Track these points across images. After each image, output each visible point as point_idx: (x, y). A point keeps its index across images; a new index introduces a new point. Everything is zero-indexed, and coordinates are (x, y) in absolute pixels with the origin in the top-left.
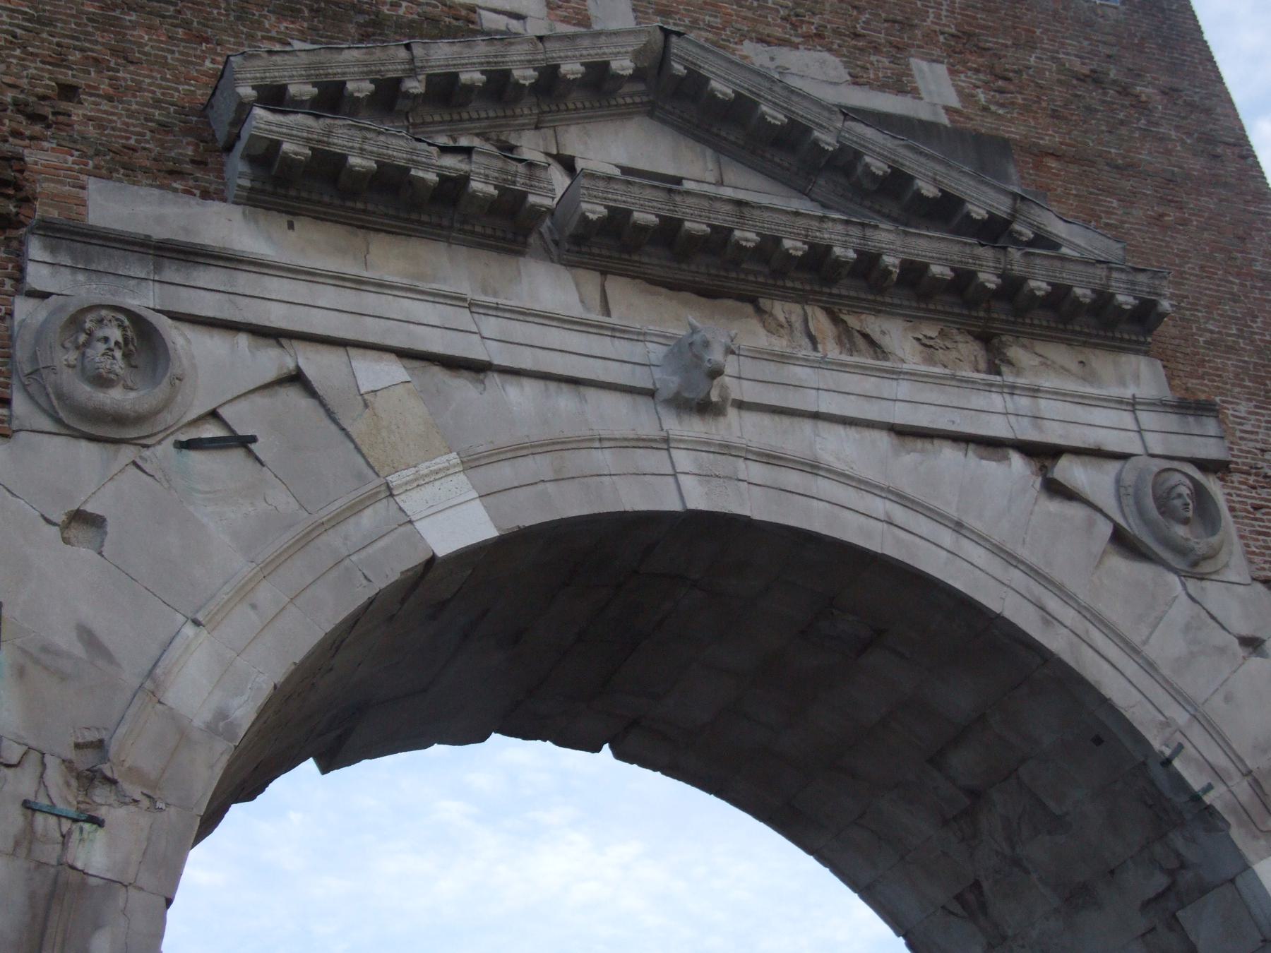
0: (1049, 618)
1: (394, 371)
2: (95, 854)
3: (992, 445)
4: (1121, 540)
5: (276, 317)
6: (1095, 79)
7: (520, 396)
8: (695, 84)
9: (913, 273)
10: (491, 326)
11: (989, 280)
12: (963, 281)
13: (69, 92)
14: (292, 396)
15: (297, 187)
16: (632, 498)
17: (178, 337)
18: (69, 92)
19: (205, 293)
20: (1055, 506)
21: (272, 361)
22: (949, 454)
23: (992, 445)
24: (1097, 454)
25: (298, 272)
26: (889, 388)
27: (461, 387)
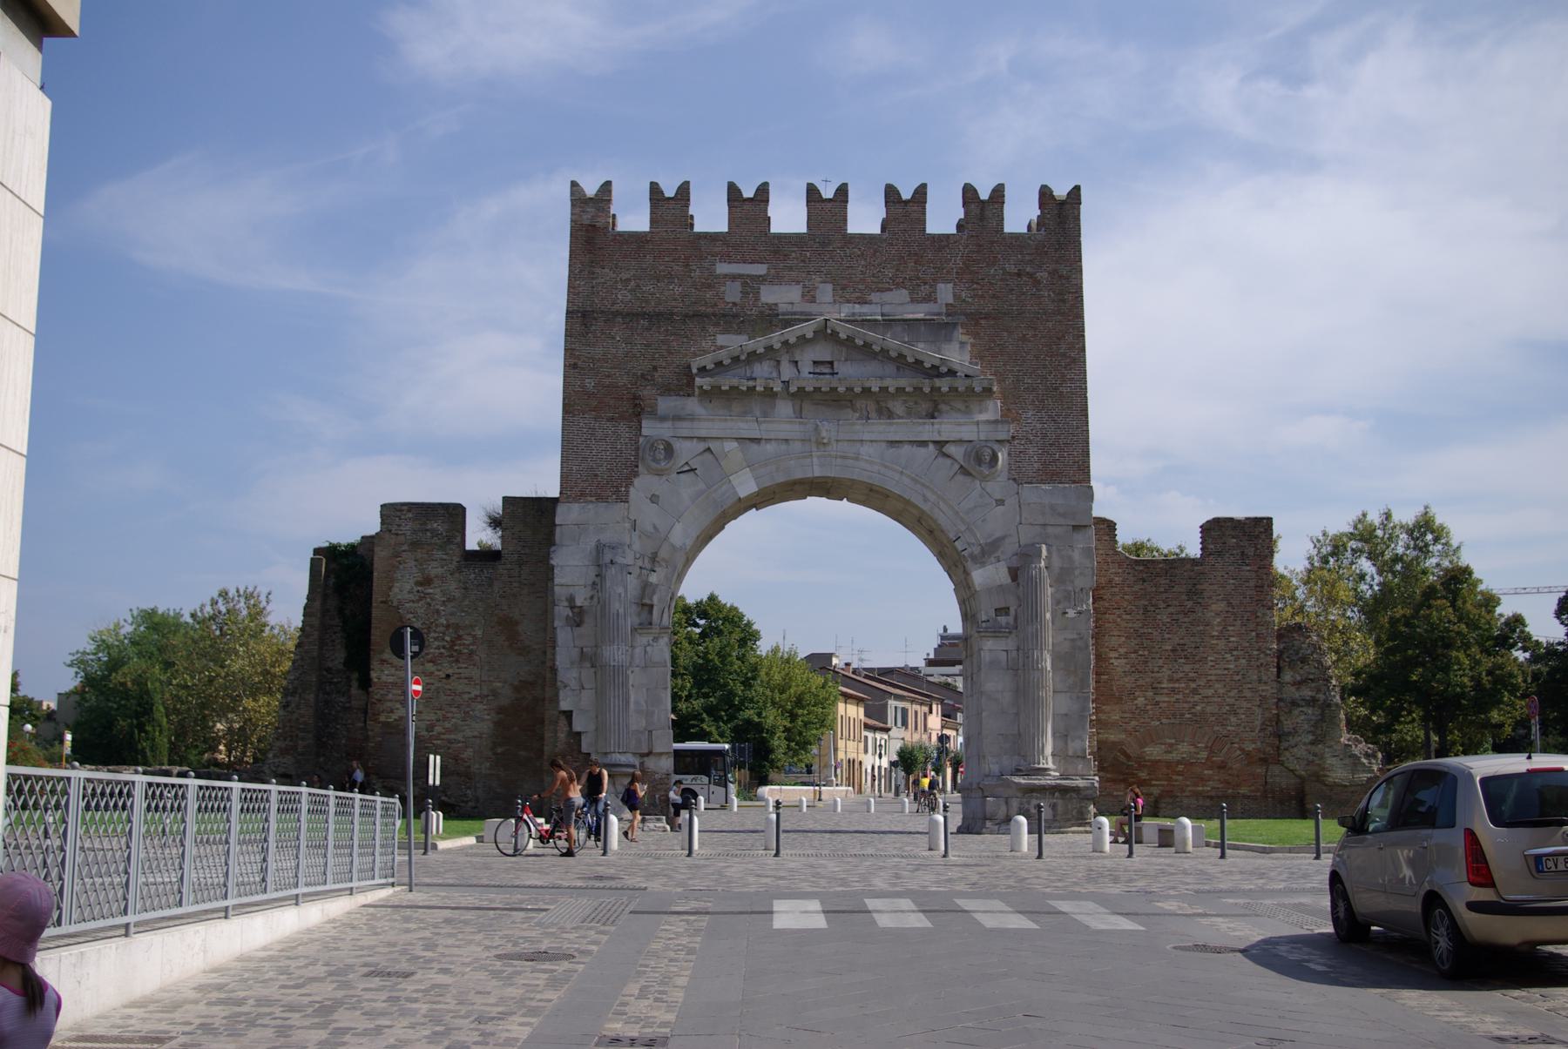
0: (926, 500)
1: (735, 444)
2: (653, 578)
3: (923, 444)
4: (964, 471)
5: (703, 433)
6: (1019, 275)
7: (770, 448)
8: (835, 334)
9: (900, 390)
10: (764, 426)
11: (927, 390)
12: (918, 389)
13: (655, 368)
14: (708, 456)
15: (708, 395)
16: (798, 475)
17: (677, 445)
18: (655, 368)
19: (685, 428)
20: (941, 460)
21: (702, 446)
22: (907, 448)
23: (923, 444)
24: (960, 442)
25: (710, 422)
26: (892, 428)
27: (754, 447)
